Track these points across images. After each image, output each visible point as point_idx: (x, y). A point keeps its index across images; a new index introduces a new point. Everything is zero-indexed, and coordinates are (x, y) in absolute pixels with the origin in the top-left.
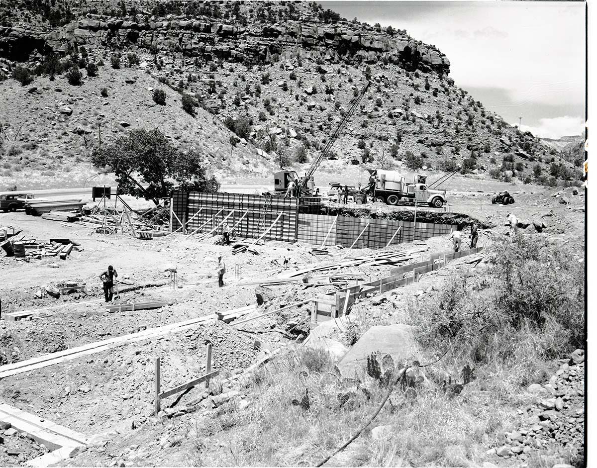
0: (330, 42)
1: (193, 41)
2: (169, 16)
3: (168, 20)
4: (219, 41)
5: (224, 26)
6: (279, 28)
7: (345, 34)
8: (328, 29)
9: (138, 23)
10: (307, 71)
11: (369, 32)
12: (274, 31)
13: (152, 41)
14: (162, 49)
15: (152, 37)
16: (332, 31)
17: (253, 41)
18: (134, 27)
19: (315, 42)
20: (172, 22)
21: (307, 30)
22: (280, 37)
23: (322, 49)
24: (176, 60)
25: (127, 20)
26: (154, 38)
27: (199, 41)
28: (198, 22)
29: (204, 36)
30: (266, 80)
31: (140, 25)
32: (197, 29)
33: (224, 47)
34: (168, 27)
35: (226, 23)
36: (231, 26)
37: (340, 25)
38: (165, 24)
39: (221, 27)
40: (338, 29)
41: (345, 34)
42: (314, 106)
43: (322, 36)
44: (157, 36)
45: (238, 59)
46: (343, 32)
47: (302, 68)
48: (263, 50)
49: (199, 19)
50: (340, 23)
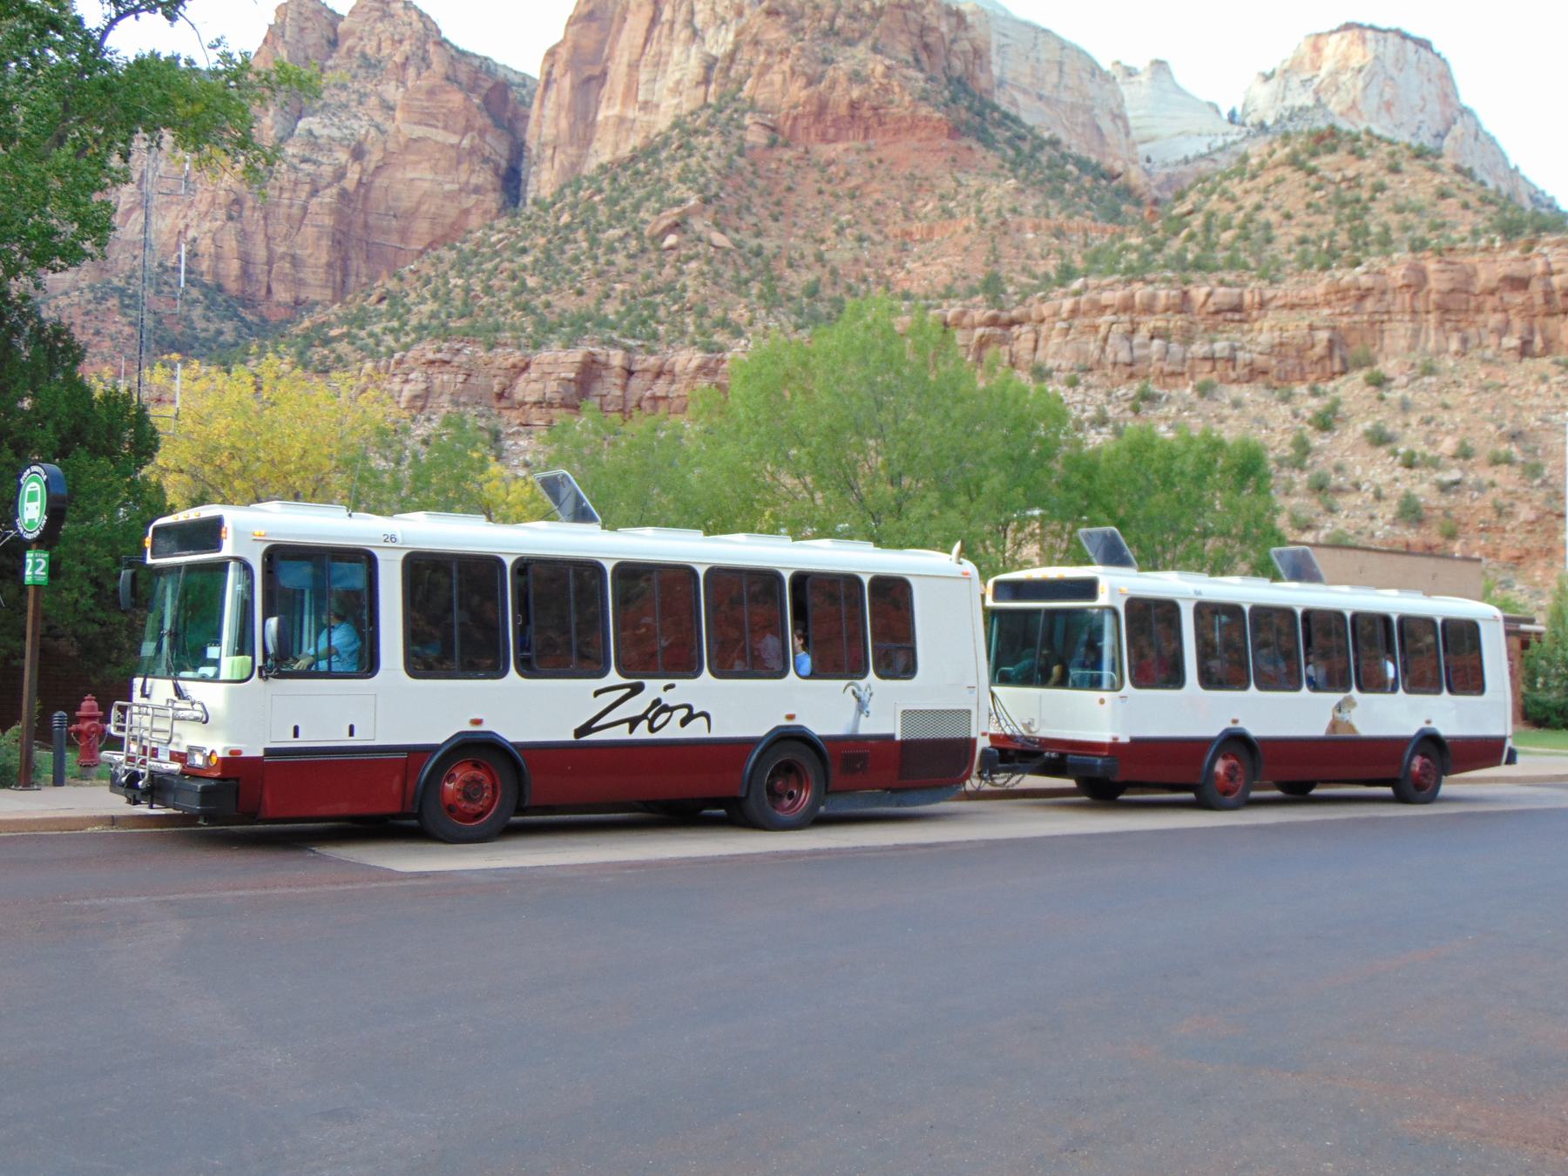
0: (1518, 298)
1: (1137, 340)
2: (1077, 284)
3: (1077, 293)
4: (1206, 330)
5: (1221, 290)
6: (1366, 281)
7: (1560, 272)
8: (1507, 261)
9: (1001, 309)
10: (1446, 385)
13: (1035, 349)
14: (1058, 370)
15: (1036, 341)
17: (1295, 326)
18: (993, 322)
19: (1473, 304)
20: (1083, 299)
22: (1369, 305)
23: (1495, 320)
24: (1091, 392)
25: (975, 307)
26: (1041, 344)
27: (1152, 338)
28: (1150, 289)
29: (1161, 324)
30: (1325, 422)
31: (1005, 316)
33: (1221, 347)
34: (1074, 312)
35: (1222, 283)
36: (1237, 291)
37: (1546, 250)
38: (1068, 304)
39: (1209, 295)
41: (1560, 272)
42: (1456, 483)
43: (1493, 284)
44: (1047, 339)
45: (1255, 373)
47: (1433, 379)
48: (1325, 343)
49: (1152, 282)
50: (1547, 244)
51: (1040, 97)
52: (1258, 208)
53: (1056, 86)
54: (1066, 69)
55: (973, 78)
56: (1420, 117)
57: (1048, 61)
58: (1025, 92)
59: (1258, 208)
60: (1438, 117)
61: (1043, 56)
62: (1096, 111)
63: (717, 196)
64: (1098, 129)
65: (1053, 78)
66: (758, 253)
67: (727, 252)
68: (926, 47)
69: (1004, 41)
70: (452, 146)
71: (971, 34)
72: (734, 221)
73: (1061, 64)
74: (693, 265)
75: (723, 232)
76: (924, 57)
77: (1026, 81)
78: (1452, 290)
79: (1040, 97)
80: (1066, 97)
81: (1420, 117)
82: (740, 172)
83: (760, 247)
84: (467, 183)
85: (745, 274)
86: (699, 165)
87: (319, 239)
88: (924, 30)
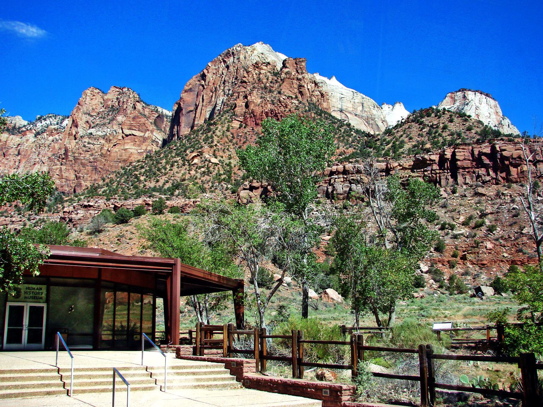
6: (433, 157)
7: (505, 150)
11: (535, 144)
12: (427, 160)
16: (488, 150)
21: (462, 153)
32: (345, 172)
40: (497, 146)
41: (505, 150)
46: (503, 148)
51: (356, 115)
52: (401, 136)
53: (361, 111)
54: (364, 105)
55: (321, 104)
56: (489, 120)
57: (358, 103)
58: (350, 113)
59: (401, 136)
60: (495, 120)
61: (356, 101)
62: (376, 119)
63: (216, 145)
64: (377, 125)
65: (360, 108)
66: (229, 165)
67: (216, 164)
68: (301, 93)
69: (342, 96)
70: (141, 137)
71: (320, 89)
72: (221, 153)
73: (363, 104)
74: (203, 169)
75: (216, 158)
76: (299, 96)
77: (350, 109)
78: (465, 159)
79: (356, 115)
80: (365, 115)
81: (489, 120)
82: (227, 137)
83: (230, 163)
84: (146, 149)
85: (222, 172)
86: (211, 135)
87: (92, 171)
88: (300, 86)
